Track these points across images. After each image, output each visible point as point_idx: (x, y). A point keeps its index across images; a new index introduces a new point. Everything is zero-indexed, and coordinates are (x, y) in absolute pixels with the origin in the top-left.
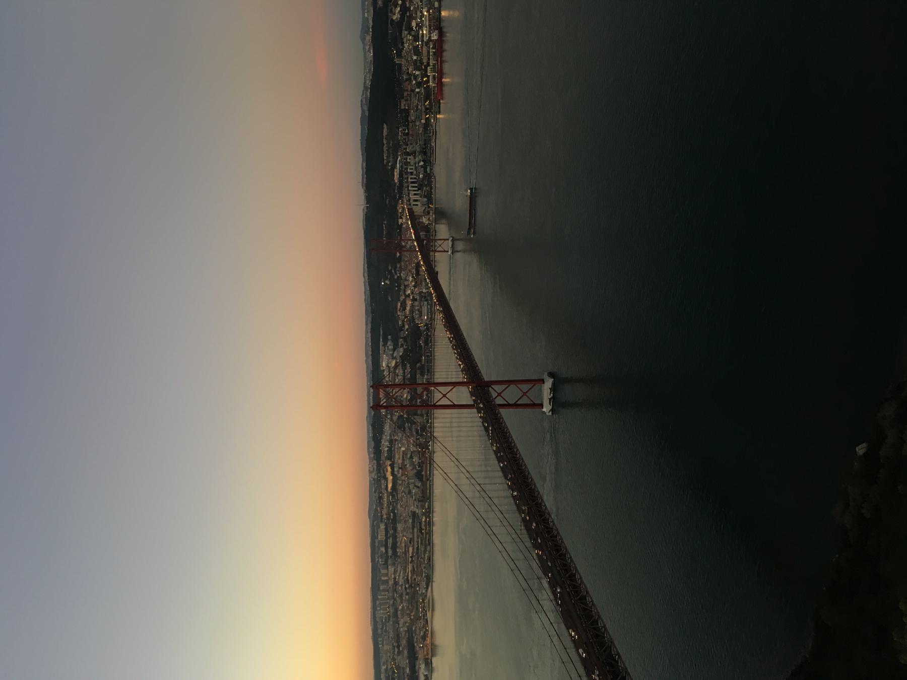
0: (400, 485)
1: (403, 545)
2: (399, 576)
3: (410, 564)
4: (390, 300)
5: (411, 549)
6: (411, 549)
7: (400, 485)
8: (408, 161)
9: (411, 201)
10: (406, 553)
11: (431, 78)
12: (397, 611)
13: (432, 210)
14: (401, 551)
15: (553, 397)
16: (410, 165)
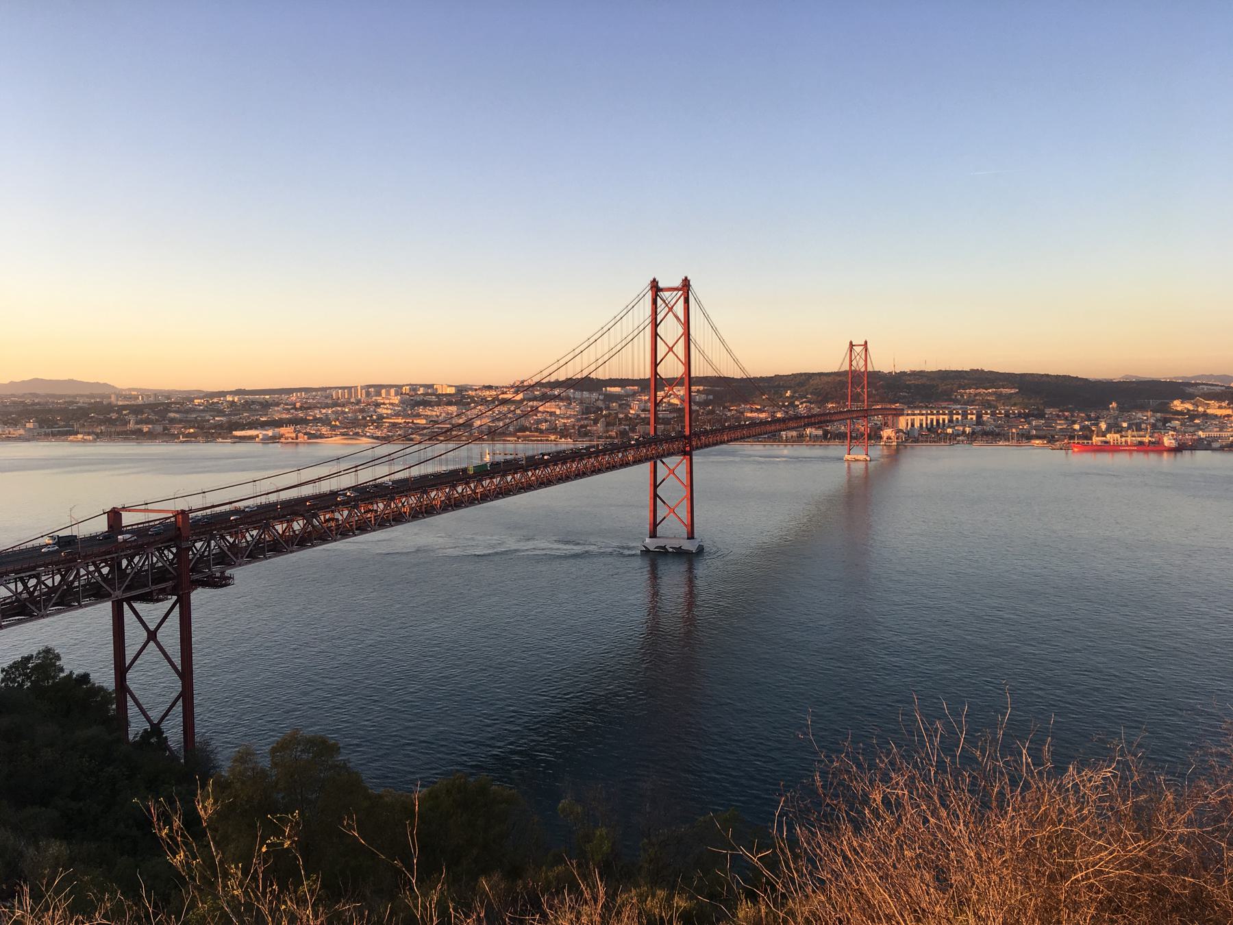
0: (509, 409)
1: (429, 413)
2: (387, 409)
3: (404, 420)
4: (764, 397)
5: (424, 421)
6: (424, 421)
7: (509, 409)
8: (969, 417)
9: (912, 417)
10: (419, 416)
11: (1104, 438)
12: (340, 406)
13: (902, 442)
14: (421, 410)
15: (667, 552)
16: (962, 419)
